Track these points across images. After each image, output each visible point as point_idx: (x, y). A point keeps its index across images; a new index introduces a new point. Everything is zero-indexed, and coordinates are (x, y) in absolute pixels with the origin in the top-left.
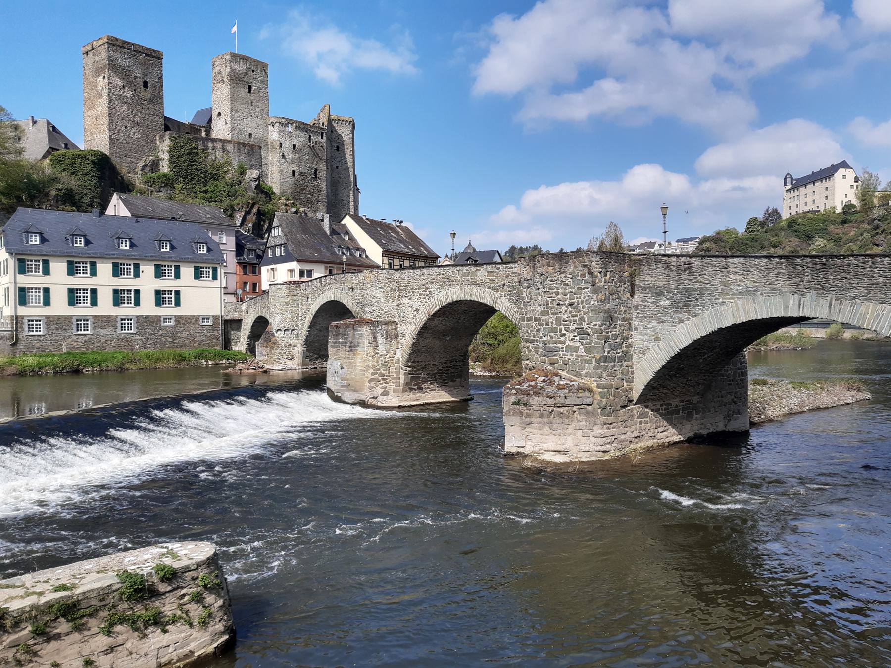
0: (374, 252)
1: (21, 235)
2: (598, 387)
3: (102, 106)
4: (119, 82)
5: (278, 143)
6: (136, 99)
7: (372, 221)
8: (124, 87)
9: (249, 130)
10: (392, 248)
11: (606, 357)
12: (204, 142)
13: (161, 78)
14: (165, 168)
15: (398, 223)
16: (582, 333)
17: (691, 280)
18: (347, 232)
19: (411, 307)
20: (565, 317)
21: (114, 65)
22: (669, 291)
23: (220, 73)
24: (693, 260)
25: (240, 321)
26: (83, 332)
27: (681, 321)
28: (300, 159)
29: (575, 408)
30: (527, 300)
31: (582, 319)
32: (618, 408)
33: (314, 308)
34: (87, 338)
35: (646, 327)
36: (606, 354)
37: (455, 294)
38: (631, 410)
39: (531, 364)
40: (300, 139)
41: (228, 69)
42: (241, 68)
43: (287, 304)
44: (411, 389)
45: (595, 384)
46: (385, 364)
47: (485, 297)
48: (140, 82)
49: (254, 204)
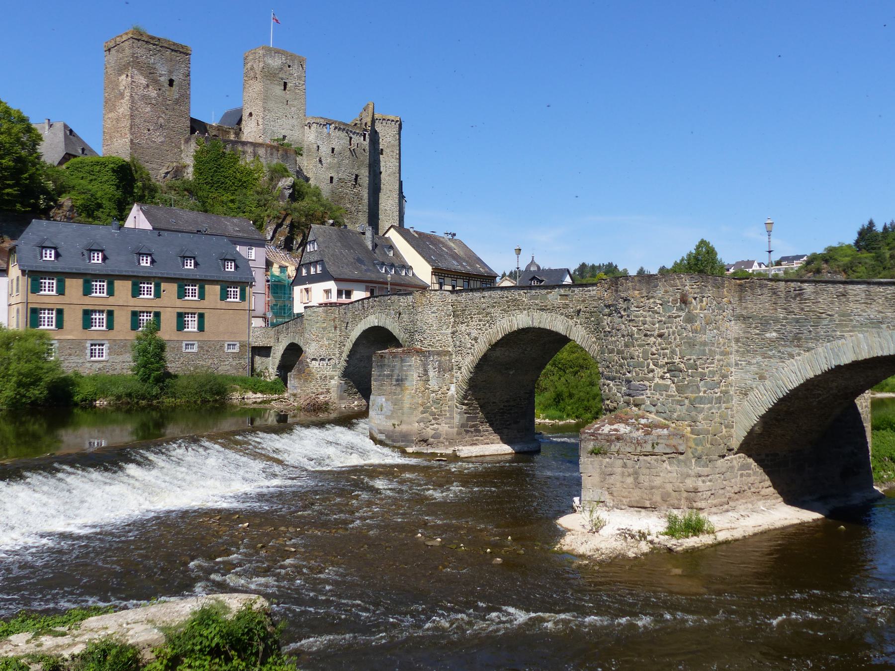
0: (422, 270)
1: (35, 250)
2: (692, 432)
3: (123, 107)
4: (143, 81)
5: (315, 146)
6: (160, 99)
7: (420, 234)
8: (148, 86)
9: (284, 132)
10: (442, 265)
11: (701, 398)
12: (233, 145)
13: (189, 75)
14: (190, 174)
15: (450, 236)
16: (673, 370)
17: (802, 309)
18: (391, 247)
19: (469, 334)
20: (654, 350)
21: (138, 63)
22: (776, 321)
24: (805, 285)
25: (270, 348)
26: (97, 358)
27: (792, 356)
28: (339, 165)
29: (664, 457)
30: (608, 329)
31: (673, 352)
32: (716, 457)
33: (356, 332)
34: (101, 365)
35: (749, 363)
36: (701, 394)
37: (521, 320)
38: (731, 461)
39: (612, 406)
40: (339, 140)
41: (261, 64)
42: (275, 62)
43: (324, 329)
44: (467, 432)
45: (689, 429)
46: (436, 401)
47: (557, 324)
48: (164, 80)
49: (287, 215)
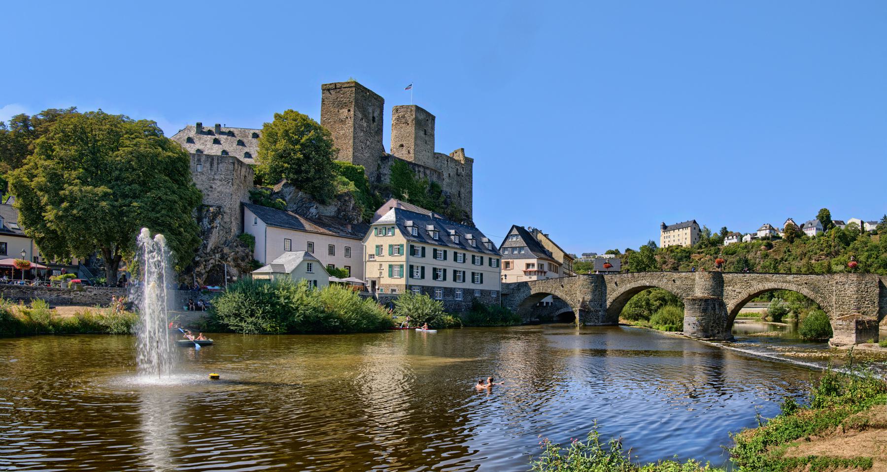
4: (360, 116)
23: (403, 117)
